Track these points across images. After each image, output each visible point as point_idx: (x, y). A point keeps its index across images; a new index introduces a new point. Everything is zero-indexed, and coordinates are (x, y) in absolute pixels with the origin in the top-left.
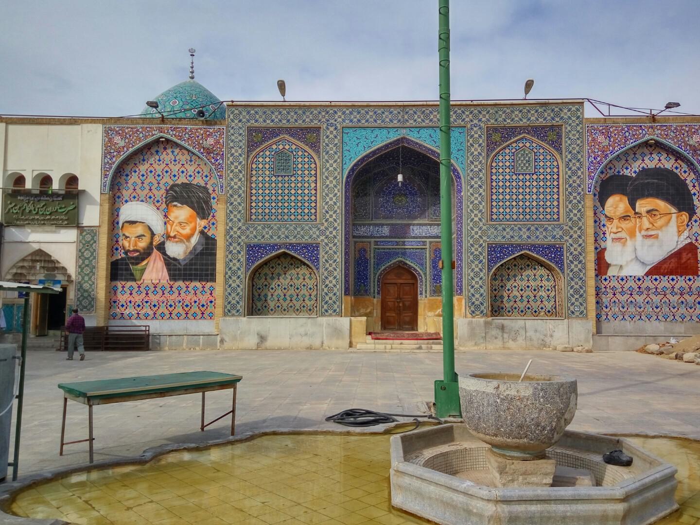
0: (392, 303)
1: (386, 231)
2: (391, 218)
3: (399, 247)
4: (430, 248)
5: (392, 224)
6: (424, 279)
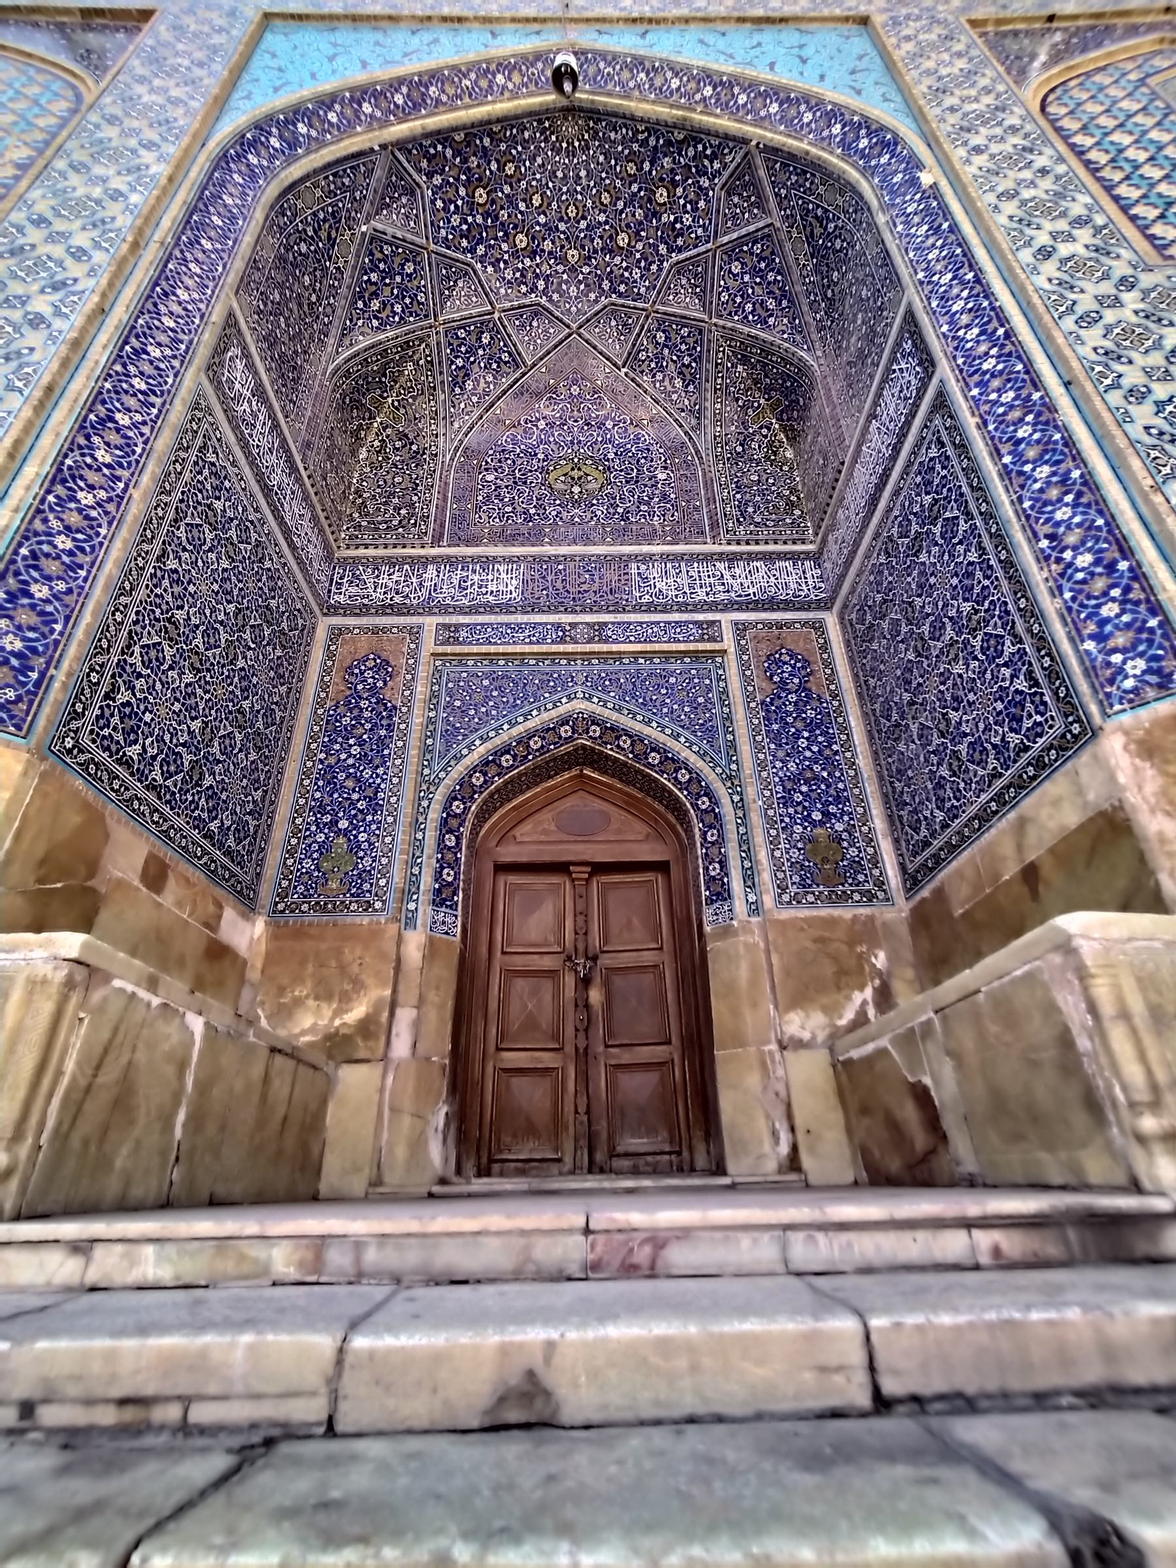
0: (547, 985)
1: (507, 583)
2: (535, 537)
3: (570, 648)
4: (742, 650)
5: (537, 559)
6: (727, 809)
